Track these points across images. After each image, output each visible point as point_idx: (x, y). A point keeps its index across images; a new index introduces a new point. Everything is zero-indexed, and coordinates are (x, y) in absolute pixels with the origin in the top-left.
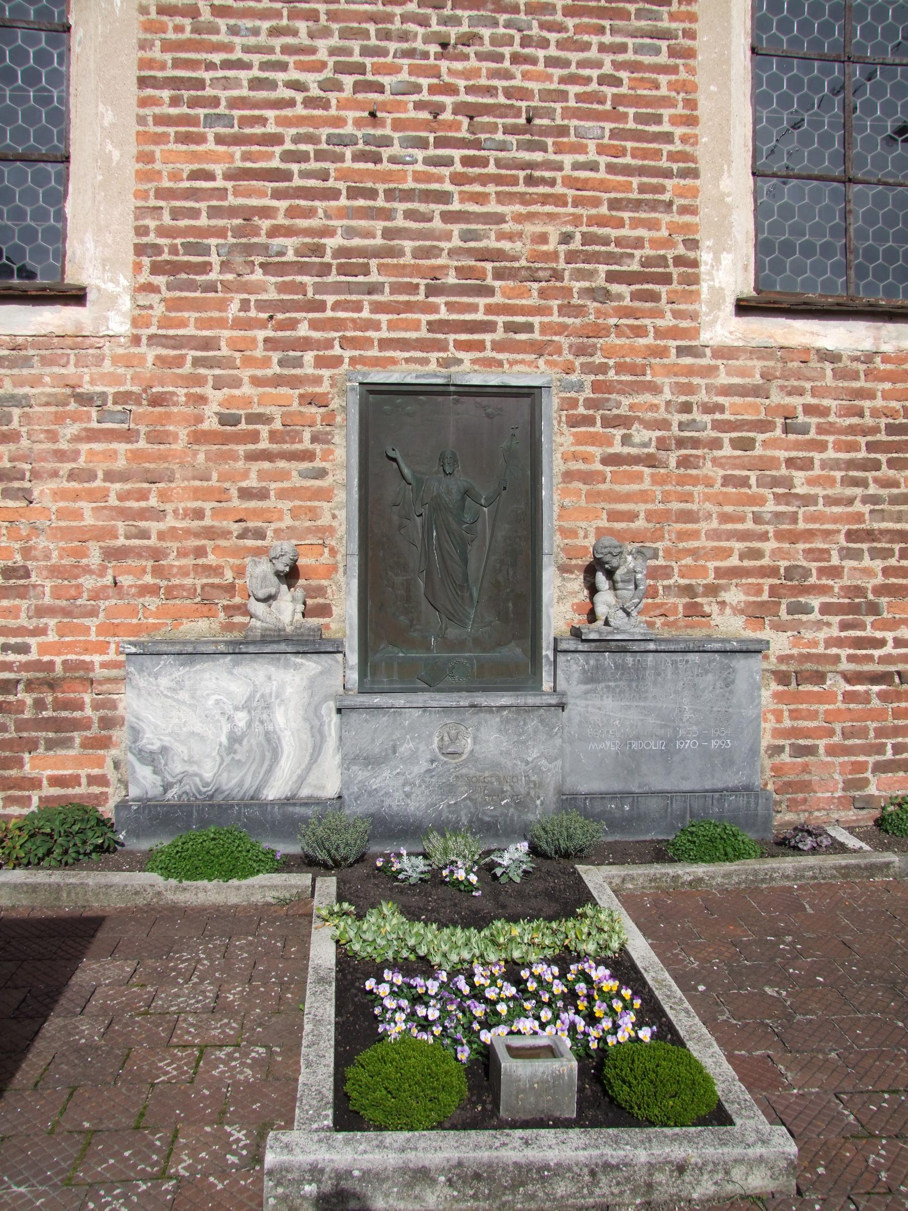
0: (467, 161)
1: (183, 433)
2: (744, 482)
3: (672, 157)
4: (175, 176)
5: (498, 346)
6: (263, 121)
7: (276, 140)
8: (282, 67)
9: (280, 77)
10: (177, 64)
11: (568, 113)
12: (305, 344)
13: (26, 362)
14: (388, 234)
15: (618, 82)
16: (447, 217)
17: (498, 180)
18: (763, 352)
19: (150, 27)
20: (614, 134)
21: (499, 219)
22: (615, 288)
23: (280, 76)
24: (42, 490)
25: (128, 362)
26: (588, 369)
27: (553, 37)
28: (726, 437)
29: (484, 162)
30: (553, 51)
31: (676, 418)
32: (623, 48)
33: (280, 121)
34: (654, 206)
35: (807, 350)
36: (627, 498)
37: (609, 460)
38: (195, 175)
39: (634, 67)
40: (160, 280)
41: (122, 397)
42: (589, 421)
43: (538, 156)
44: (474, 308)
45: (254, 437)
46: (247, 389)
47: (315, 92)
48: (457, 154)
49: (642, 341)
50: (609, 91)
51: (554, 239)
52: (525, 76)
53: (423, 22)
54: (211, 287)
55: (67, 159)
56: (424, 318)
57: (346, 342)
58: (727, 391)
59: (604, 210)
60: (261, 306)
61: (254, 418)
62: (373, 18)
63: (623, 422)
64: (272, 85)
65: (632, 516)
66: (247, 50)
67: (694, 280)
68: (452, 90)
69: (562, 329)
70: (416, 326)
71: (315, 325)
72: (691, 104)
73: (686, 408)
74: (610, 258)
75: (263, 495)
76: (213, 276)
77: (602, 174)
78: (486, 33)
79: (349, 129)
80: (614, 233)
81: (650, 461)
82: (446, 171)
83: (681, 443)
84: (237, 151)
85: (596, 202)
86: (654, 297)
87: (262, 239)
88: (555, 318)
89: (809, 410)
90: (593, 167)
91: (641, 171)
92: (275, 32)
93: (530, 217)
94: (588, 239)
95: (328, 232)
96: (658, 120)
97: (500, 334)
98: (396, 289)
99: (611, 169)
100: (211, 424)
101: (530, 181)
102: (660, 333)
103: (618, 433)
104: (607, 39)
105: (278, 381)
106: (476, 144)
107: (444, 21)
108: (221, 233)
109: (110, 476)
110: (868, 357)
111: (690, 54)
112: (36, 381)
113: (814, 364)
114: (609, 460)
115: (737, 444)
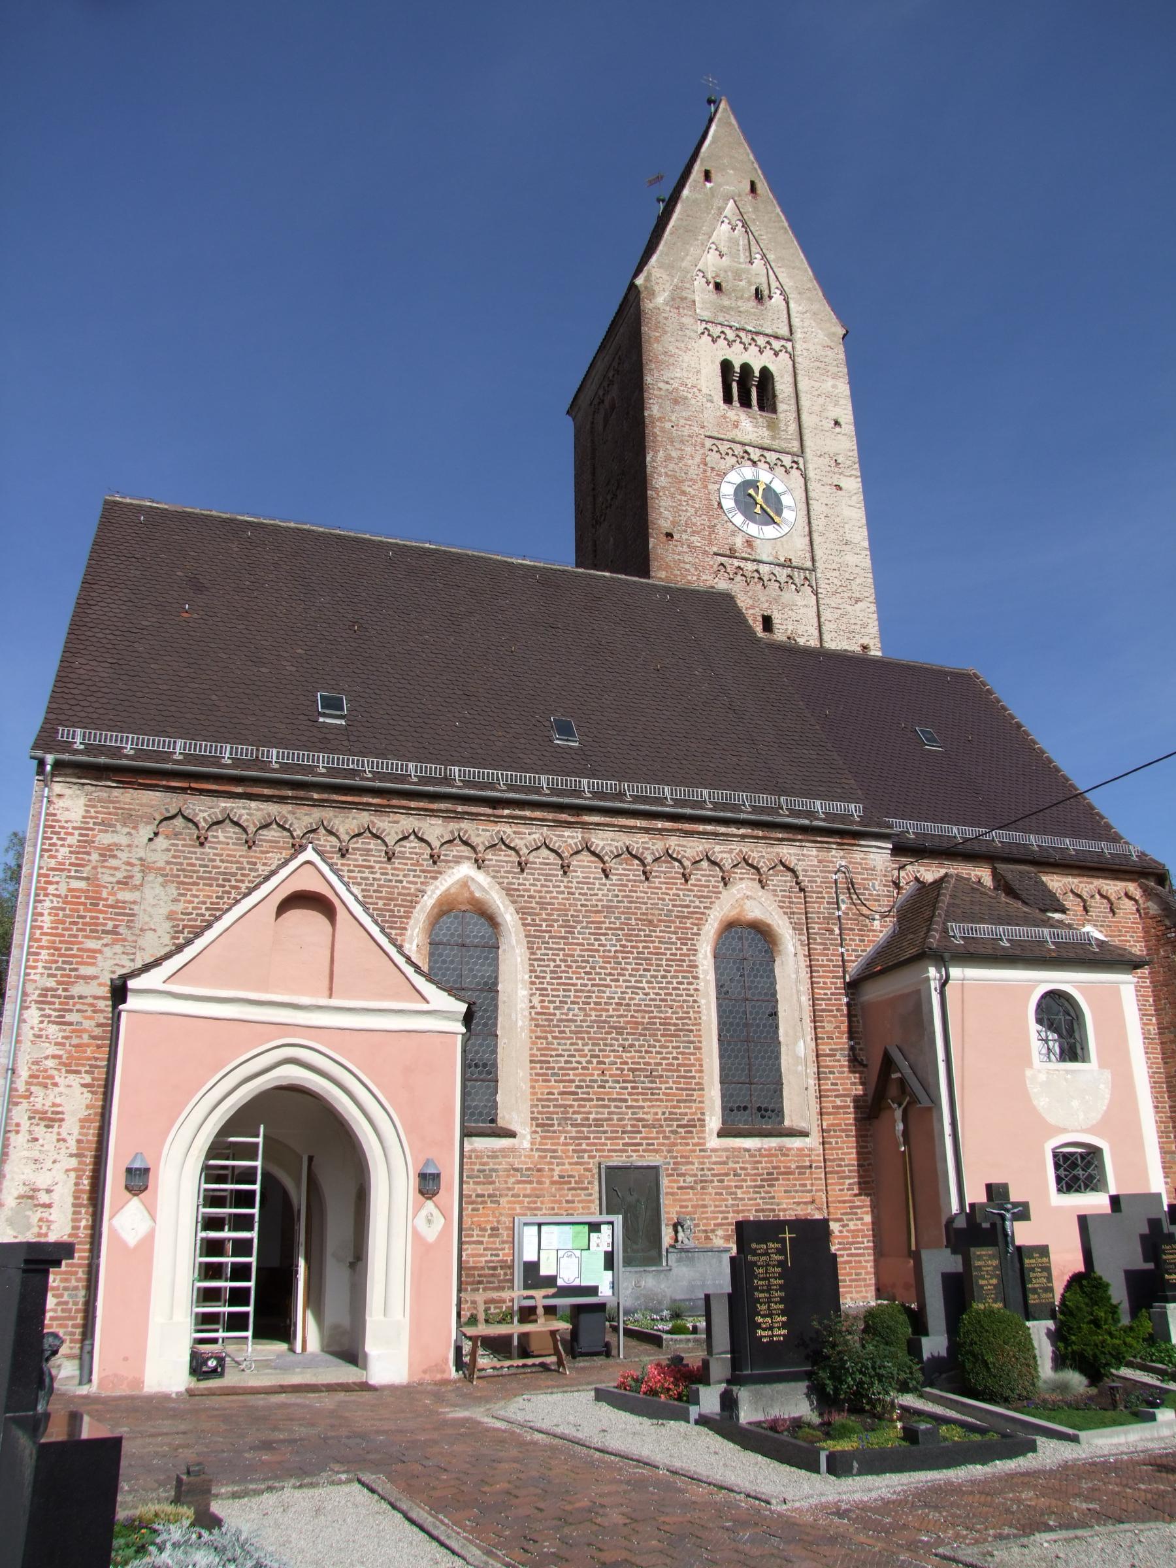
0: (633, 1088)
1: (548, 1181)
2: (721, 1194)
3: (696, 1084)
4: (542, 1094)
5: (644, 1151)
7: (573, 1081)
8: (574, 1056)
9: (574, 1059)
10: (542, 1055)
11: (664, 1070)
12: (585, 1151)
13: (497, 1157)
14: (609, 1113)
15: (677, 1059)
16: (627, 1107)
17: (642, 1094)
18: (726, 1150)
19: (534, 1043)
20: (678, 1077)
21: (643, 1107)
22: (680, 1130)
24: (503, 1201)
25: (529, 1157)
26: (672, 1157)
29: (637, 1088)
31: (700, 1173)
32: (679, 1047)
33: (575, 1075)
34: (690, 1101)
36: (685, 1200)
37: (679, 1188)
38: (549, 1093)
39: (683, 1053)
40: (539, 1129)
41: (528, 1169)
42: (672, 1175)
43: (654, 1085)
45: (570, 1183)
46: (567, 1166)
47: (584, 1064)
48: (629, 1085)
50: (676, 1062)
53: (617, 1040)
54: (554, 1132)
55: (497, 1081)
56: (621, 1142)
57: (597, 1150)
58: (715, 1163)
60: (571, 1138)
61: (569, 1176)
62: (602, 1039)
63: (683, 1175)
64: (571, 1062)
65: (687, 1207)
67: (703, 1126)
68: (626, 1063)
69: (663, 1144)
70: (618, 1144)
71: (588, 1145)
72: (701, 1065)
73: (703, 1169)
74: (677, 1120)
75: (573, 1202)
76: (555, 1128)
79: (595, 1077)
80: (678, 1111)
81: (692, 1188)
83: (701, 1181)
84: (561, 1085)
85: (672, 1101)
86: (691, 1132)
88: (661, 1141)
89: (741, 1168)
90: (671, 1088)
91: (686, 1089)
92: (572, 1044)
93: (653, 1106)
94: (671, 1113)
95: (590, 1113)
96: (690, 1071)
97: (644, 1147)
98: (612, 1132)
99: (677, 1089)
100: (556, 1178)
101: (652, 1094)
102: (694, 1145)
103: (681, 1179)
105: (577, 1163)
106: (635, 1082)
107: (625, 1040)
108: (557, 1113)
109: (525, 1196)
110: (760, 1150)
111: (700, 1048)
112: (500, 1164)
114: (679, 1188)
115: (719, 1181)
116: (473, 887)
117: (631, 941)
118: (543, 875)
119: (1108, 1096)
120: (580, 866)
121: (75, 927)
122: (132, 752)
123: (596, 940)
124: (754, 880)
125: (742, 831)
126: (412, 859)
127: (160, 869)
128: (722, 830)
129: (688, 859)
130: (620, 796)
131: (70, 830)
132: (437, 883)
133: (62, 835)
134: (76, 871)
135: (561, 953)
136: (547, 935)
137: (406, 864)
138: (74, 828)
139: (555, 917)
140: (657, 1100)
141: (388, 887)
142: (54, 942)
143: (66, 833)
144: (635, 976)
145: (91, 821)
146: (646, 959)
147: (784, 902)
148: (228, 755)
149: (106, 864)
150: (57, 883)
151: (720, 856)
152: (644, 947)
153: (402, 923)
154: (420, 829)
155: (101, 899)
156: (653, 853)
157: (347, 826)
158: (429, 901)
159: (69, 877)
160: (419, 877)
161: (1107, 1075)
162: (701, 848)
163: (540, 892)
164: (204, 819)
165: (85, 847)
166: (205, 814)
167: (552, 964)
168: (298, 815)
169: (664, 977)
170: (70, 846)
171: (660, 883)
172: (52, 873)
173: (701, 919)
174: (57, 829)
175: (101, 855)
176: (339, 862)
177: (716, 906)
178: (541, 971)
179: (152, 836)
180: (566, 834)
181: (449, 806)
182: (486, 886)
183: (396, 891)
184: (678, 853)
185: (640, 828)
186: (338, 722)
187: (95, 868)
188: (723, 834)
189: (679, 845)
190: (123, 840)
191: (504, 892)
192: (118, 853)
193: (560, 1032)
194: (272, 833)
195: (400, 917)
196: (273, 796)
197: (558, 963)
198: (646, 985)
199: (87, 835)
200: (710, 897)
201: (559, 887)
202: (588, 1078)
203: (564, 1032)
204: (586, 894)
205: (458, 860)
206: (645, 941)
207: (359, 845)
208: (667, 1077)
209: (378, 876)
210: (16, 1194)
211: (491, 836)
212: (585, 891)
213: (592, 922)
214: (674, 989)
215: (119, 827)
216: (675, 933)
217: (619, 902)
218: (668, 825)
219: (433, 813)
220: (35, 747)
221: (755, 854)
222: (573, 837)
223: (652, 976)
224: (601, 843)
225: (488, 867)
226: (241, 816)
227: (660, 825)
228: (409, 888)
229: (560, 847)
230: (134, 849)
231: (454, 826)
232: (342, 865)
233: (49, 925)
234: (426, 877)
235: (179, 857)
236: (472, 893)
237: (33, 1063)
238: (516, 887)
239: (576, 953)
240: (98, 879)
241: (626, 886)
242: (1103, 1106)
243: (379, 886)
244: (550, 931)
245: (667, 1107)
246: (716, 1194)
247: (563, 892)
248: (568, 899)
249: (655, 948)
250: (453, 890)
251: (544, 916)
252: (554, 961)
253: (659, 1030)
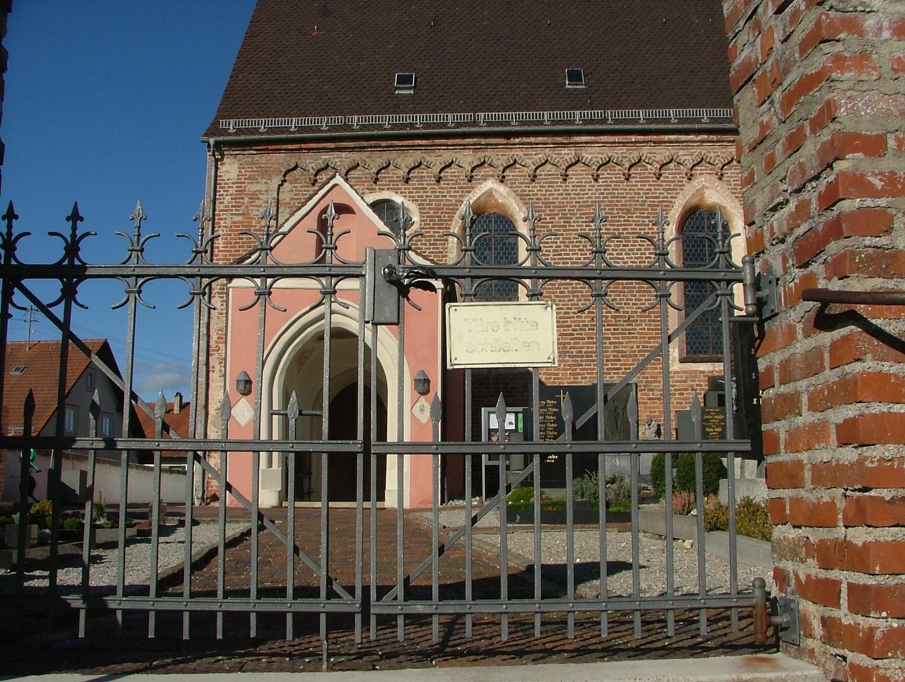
0: (615, 329)
6: (567, 322)
7: (571, 326)
12: (579, 374)
16: (610, 343)
21: (622, 343)
23: (571, 311)
26: (644, 378)
27: (634, 298)
28: (677, 392)
29: (618, 330)
30: (634, 302)
33: (571, 322)
35: (696, 371)
36: (653, 408)
37: (649, 399)
43: (631, 327)
44: (617, 365)
48: (612, 328)
51: (635, 347)
52: (628, 308)
58: (677, 382)
59: (647, 340)
60: (569, 365)
64: (569, 313)
65: (655, 412)
66: (563, 305)
77: (646, 331)
78: (618, 298)
79: (587, 323)
80: (649, 345)
82: (610, 332)
85: (645, 338)
87: (568, 350)
89: (697, 385)
90: (644, 329)
92: (569, 301)
94: (643, 347)
99: (648, 329)
101: (629, 333)
103: (651, 393)
104: (647, 298)
113: (698, 374)
114: (649, 399)
116: (496, 197)
117: (614, 225)
118: (547, 183)
120: (574, 175)
121: (237, 246)
122: (390, 126)
123: (586, 226)
124: (712, 174)
125: (700, 137)
126: (453, 180)
127: (287, 203)
128: (683, 138)
129: (657, 162)
130: (604, 121)
131: (231, 185)
132: (471, 195)
133: (226, 189)
134: (236, 210)
135: (561, 237)
136: (550, 225)
137: (449, 184)
138: (232, 183)
139: (556, 212)
140: (633, 338)
141: (437, 201)
142: (226, 255)
143: (228, 187)
144: (617, 250)
145: (243, 178)
146: (625, 238)
147: (736, 189)
148: (231, 127)
149: (254, 204)
150: (225, 219)
151: (683, 158)
152: (623, 229)
153: (446, 224)
154: (457, 159)
155: (252, 226)
156: (630, 161)
157: (406, 162)
159: (232, 214)
160: (458, 192)
162: (668, 154)
163: (545, 195)
164: (312, 167)
165: (240, 195)
166: (313, 165)
167: (554, 245)
168: (373, 159)
169: (638, 250)
170: (231, 195)
171: (636, 182)
172: (221, 213)
173: (668, 206)
174: (223, 185)
175: (249, 198)
176: (403, 187)
177: (680, 196)
178: (546, 251)
179: (280, 183)
180: (563, 152)
181: (475, 140)
182: (506, 194)
183: (442, 203)
184: (650, 158)
185: (619, 143)
186: (408, 92)
187: (247, 207)
188: (684, 142)
189: (650, 153)
190: (263, 188)
191: (518, 197)
192: (261, 196)
193: (560, 293)
194: (358, 172)
195: (445, 221)
196: (355, 148)
197: (559, 244)
198: (625, 257)
199: (241, 187)
200: (676, 189)
201: (559, 190)
202: (581, 324)
203: (563, 292)
204: (579, 194)
205: (485, 178)
206: (624, 225)
207: (416, 175)
208: (641, 321)
209: (429, 194)
210: (215, 407)
211: (508, 159)
212: (579, 191)
213: (584, 214)
214: (646, 258)
215: (259, 179)
216: (648, 217)
217: (604, 198)
218: (640, 138)
219: (464, 147)
220: (205, 135)
221: (712, 155)
222: (568, 154)
223: (629, 250)
224: (590, 157)
225: (507, 181)
226: (335, 163)
227: (633, 138)
228: (451, 201)
229: (558, 162)
230: (270, 193)
231: (480, 154)
232: (405, 189)
233: (222, 245)
234: (462, 192)
235: (299, 194)
236: (496, 200)
237: (219, 330)
238: (527, 193)
239: (572, 237)
240: (249, 214)
241: (611, 186)
243: (430, 200)
244: (553, 222)
245: (640, 342)
246: (677, 403)
247: (562, 194)
248: (565, 199)
249: (632, 229)
250: (482, 199)
251: (548, 212)
252: (556, 243)
253: (635, 288)
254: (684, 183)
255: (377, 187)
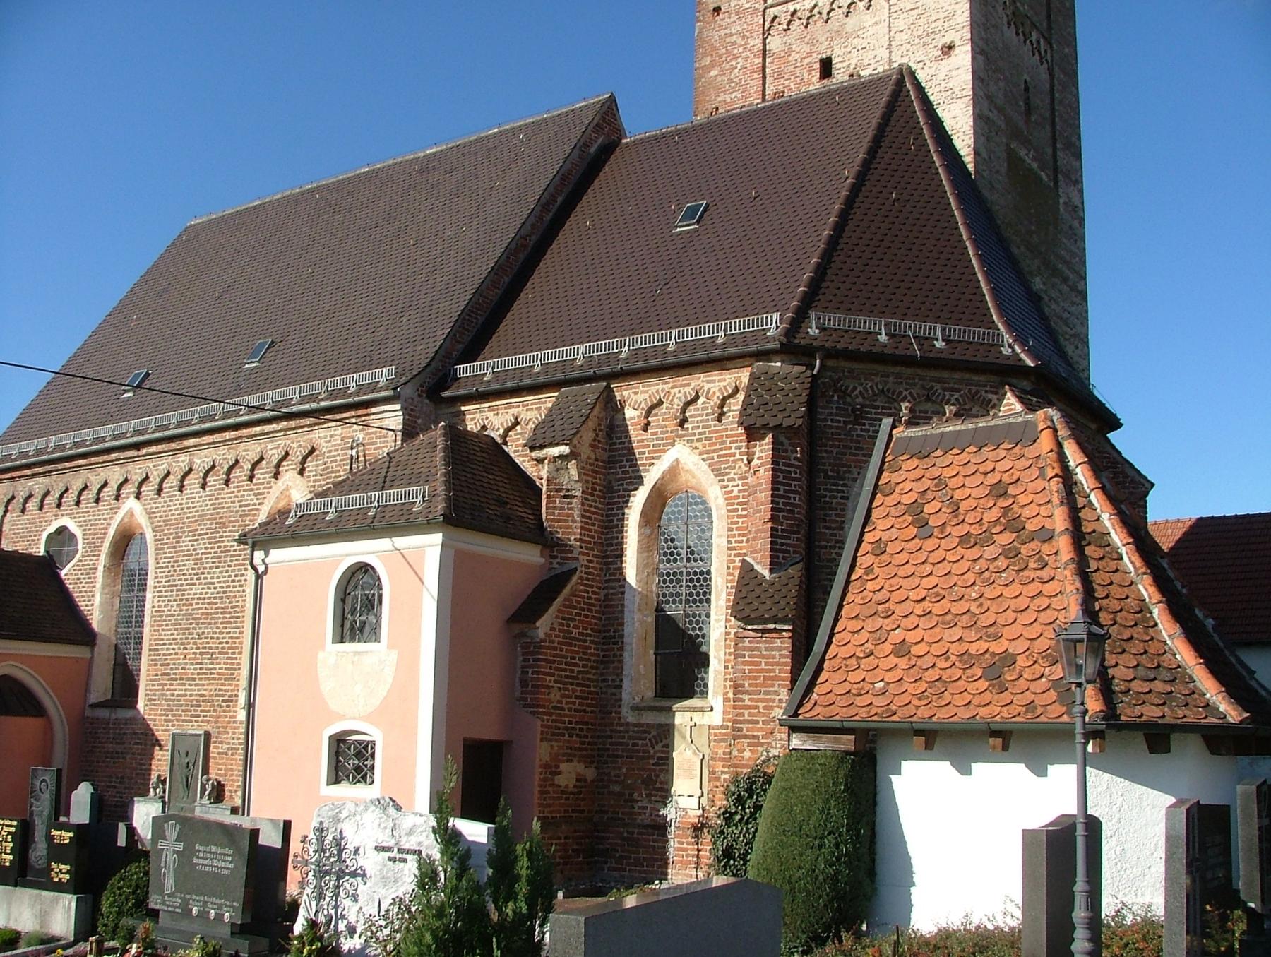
49: (226, 719)
80: (223, 688)
81: (226, 754)
94: (220, 690)
119: (390, 680)
158: (111, 532)
161: (394, 655)
177: (266, 501)
180: (181, 459)
218: (233, 434)
227: (227, 435)
242: (383, 690)
250: (126, 520)
254: (272, 484)
255: (60, 513)
